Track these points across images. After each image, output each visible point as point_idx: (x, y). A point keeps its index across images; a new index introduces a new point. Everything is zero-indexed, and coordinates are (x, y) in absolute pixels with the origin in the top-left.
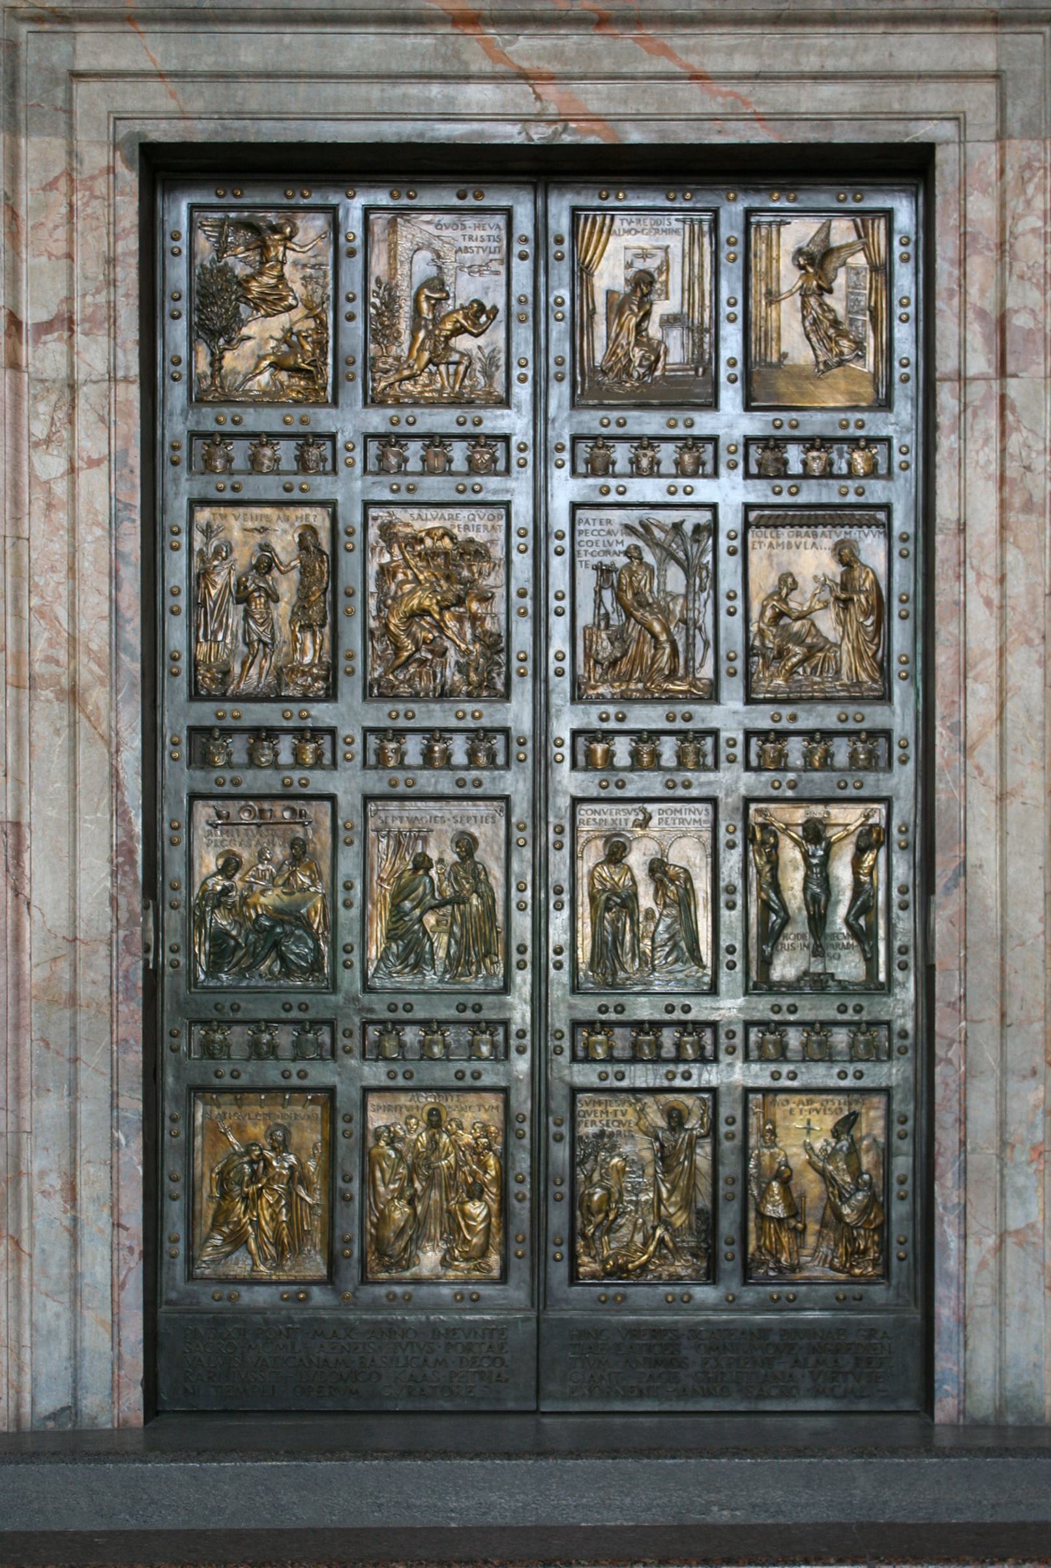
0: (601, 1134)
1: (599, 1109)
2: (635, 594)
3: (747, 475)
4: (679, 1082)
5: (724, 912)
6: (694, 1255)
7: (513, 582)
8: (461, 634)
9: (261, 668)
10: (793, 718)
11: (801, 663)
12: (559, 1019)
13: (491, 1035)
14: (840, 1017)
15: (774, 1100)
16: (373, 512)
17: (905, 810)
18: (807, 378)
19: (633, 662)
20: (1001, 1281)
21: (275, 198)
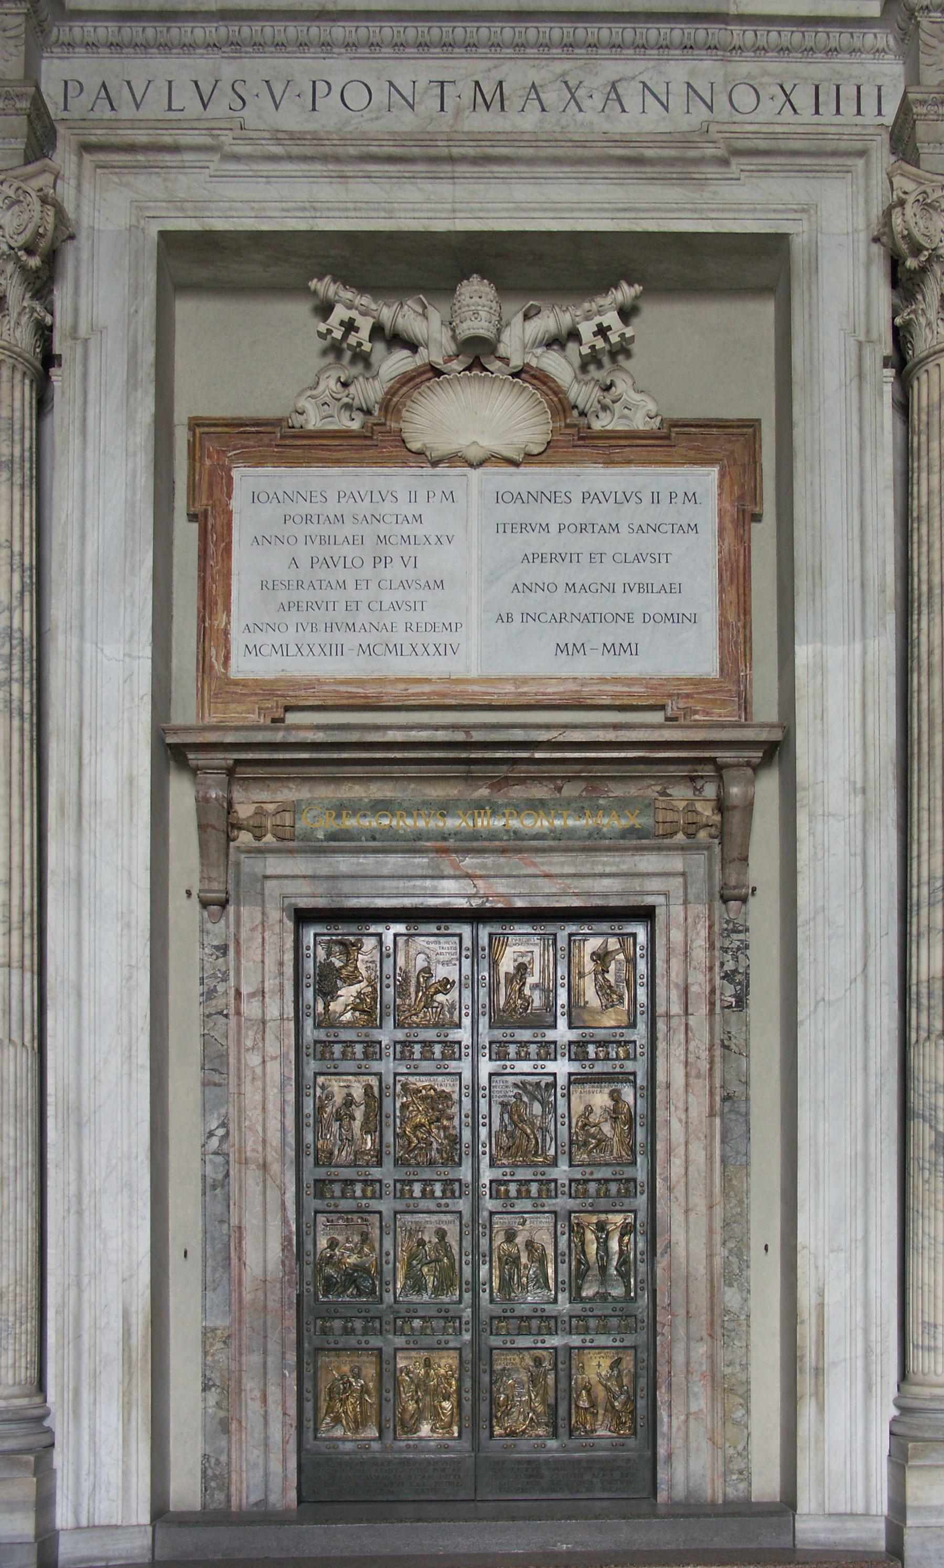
0: (504, 1369)
3: (570, 1059)
4: (539, 1345)
5: (560, 1264)
10: (592, 1173)
11: (594, 1147)
12: (484, 1316)
16: (398, 1078)
17: (642, 1216)
19: (518, 1148)
20: (687, 1436)
21: (353, 929)
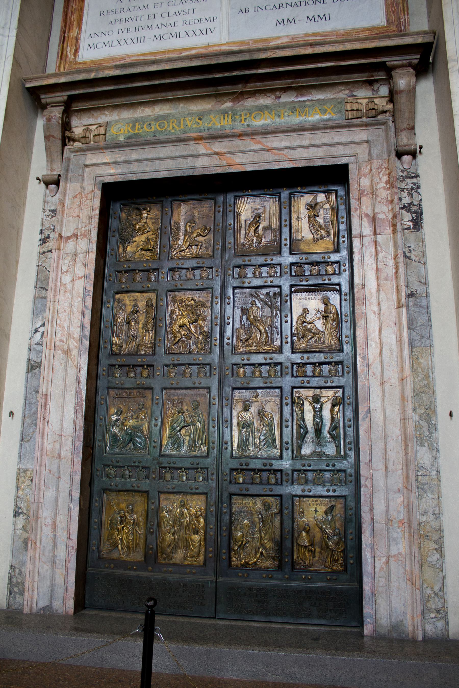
0: (240, 512)
2: (254, 317)
5: (285, 429)
6: (274, 559)
7: (213, 314)
8: (196, 332)
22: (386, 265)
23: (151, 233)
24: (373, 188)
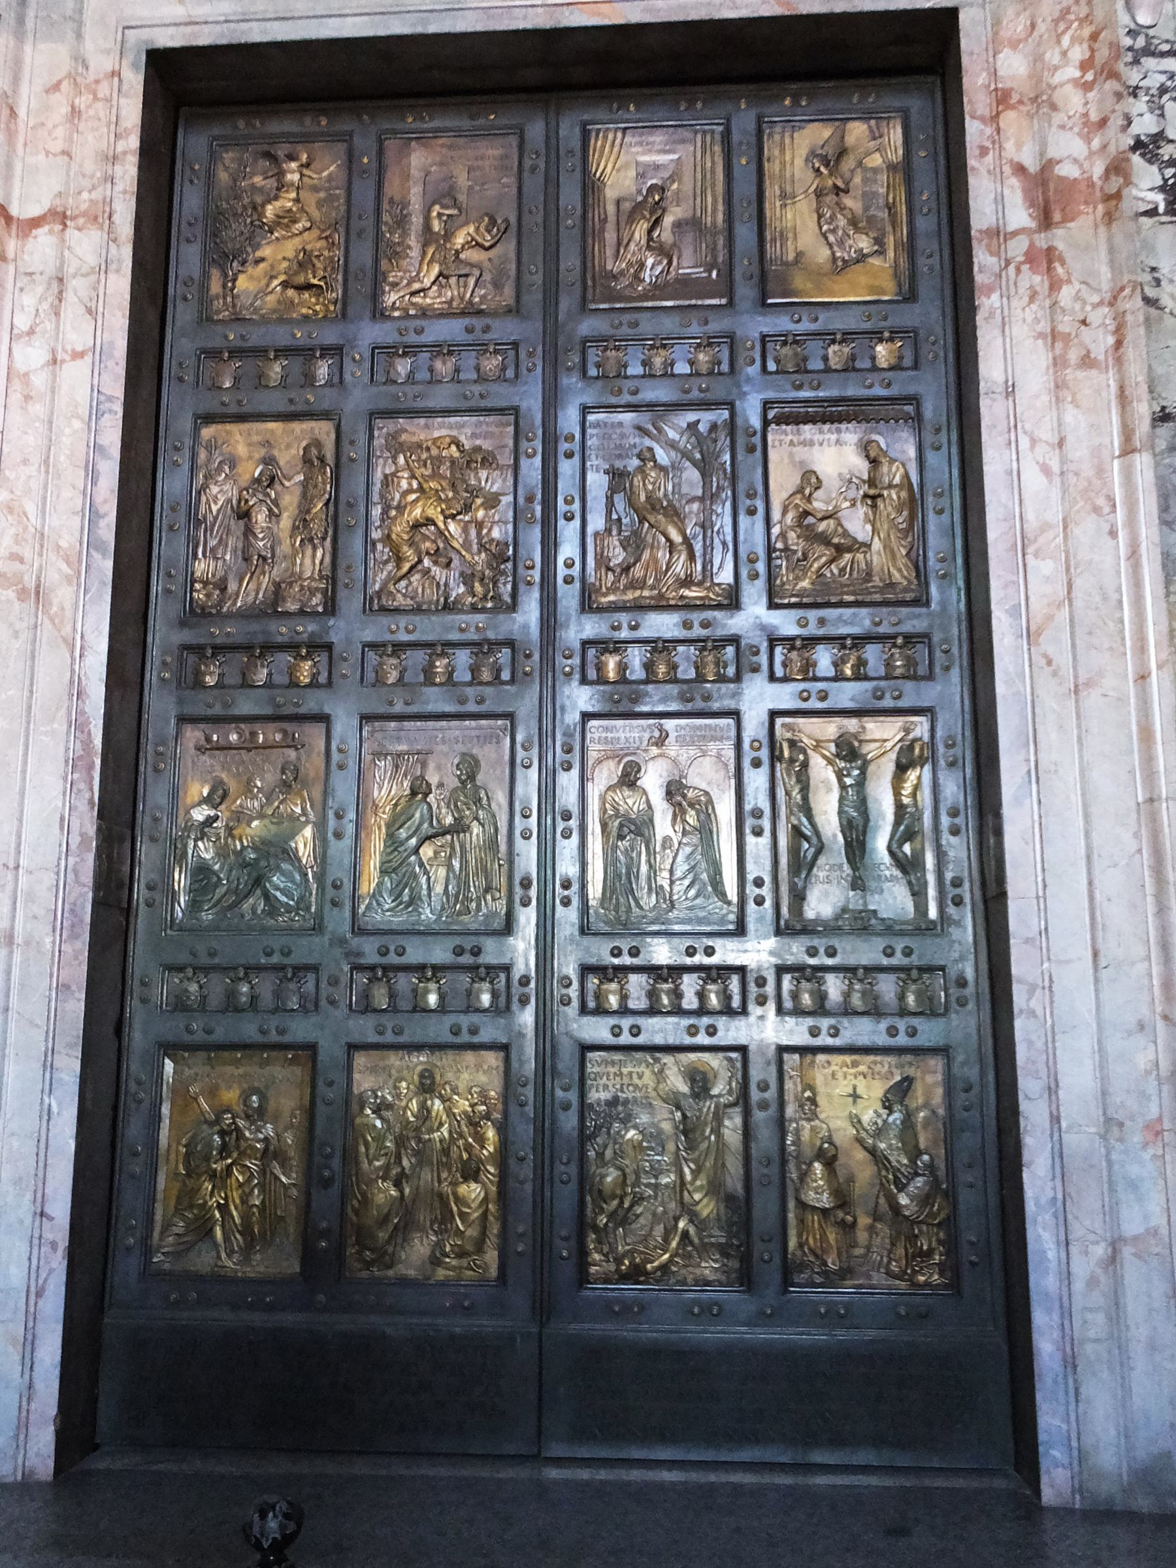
0: (614, 1102)
1: (612, 1070)
4: (702, 1039)
5: (750, 839)
9: (259, 585)
12: (567, 965)
13: (491, 982)
14: (885, 961)
15: (813, 1062)
16: (379, 423)
18: (825, 275)
22: (1084, 322)
23: (315, 233)
24: (1040, 80)
